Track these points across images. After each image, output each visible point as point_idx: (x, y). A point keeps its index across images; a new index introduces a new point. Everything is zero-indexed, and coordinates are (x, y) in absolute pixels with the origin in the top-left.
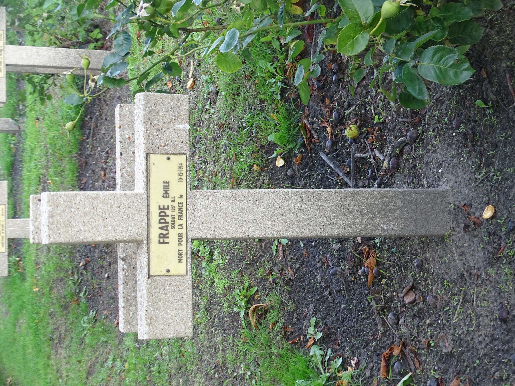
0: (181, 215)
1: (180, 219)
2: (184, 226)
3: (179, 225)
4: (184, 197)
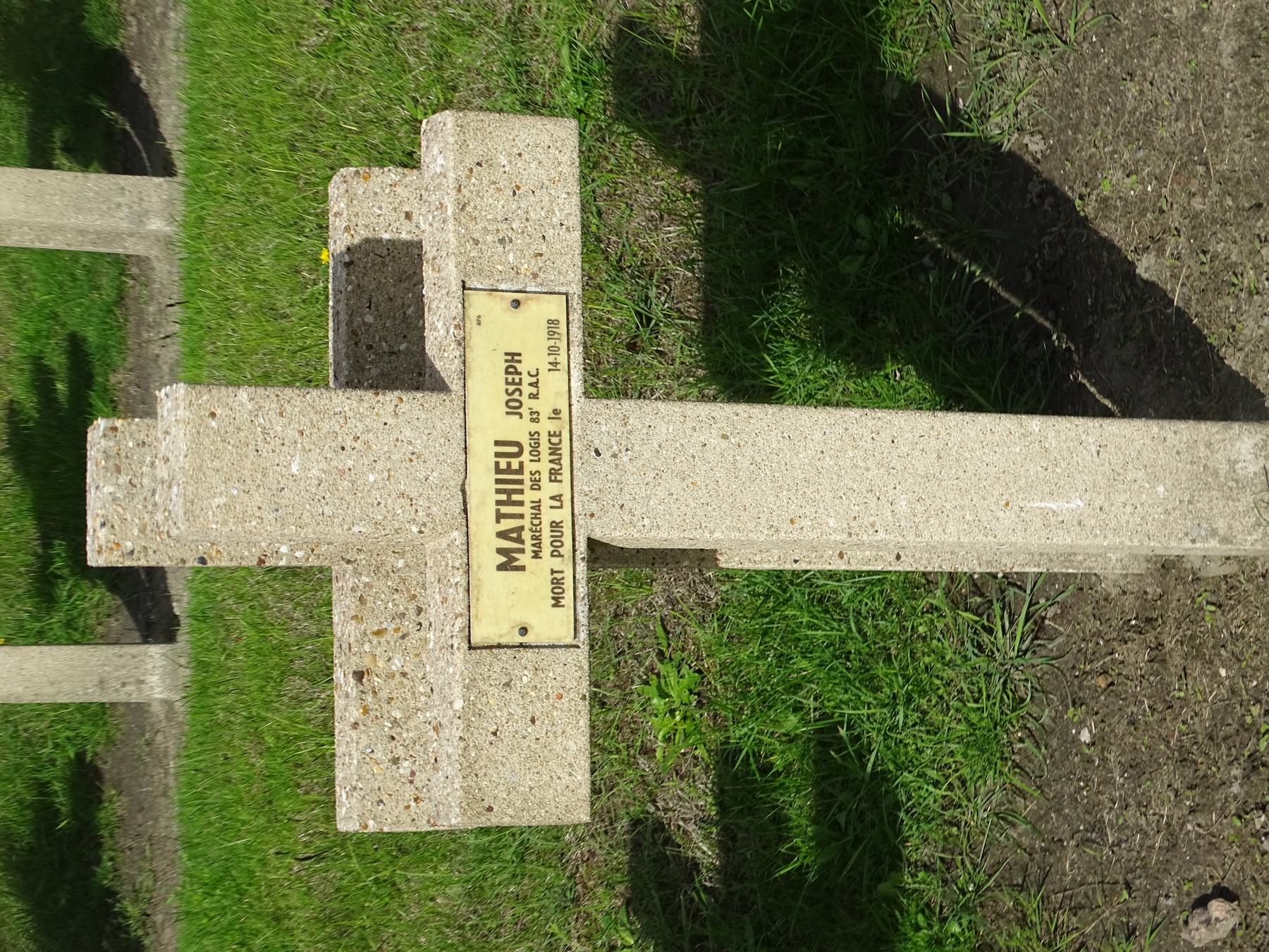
0: (557, 467)
1: (556, 481)
2: (566, 499)
3: (552, 498)
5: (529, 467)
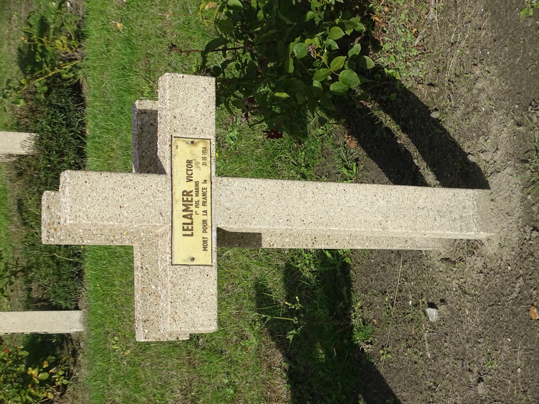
1: (205, 205)
3: (203, 212)
5: (195, 199)
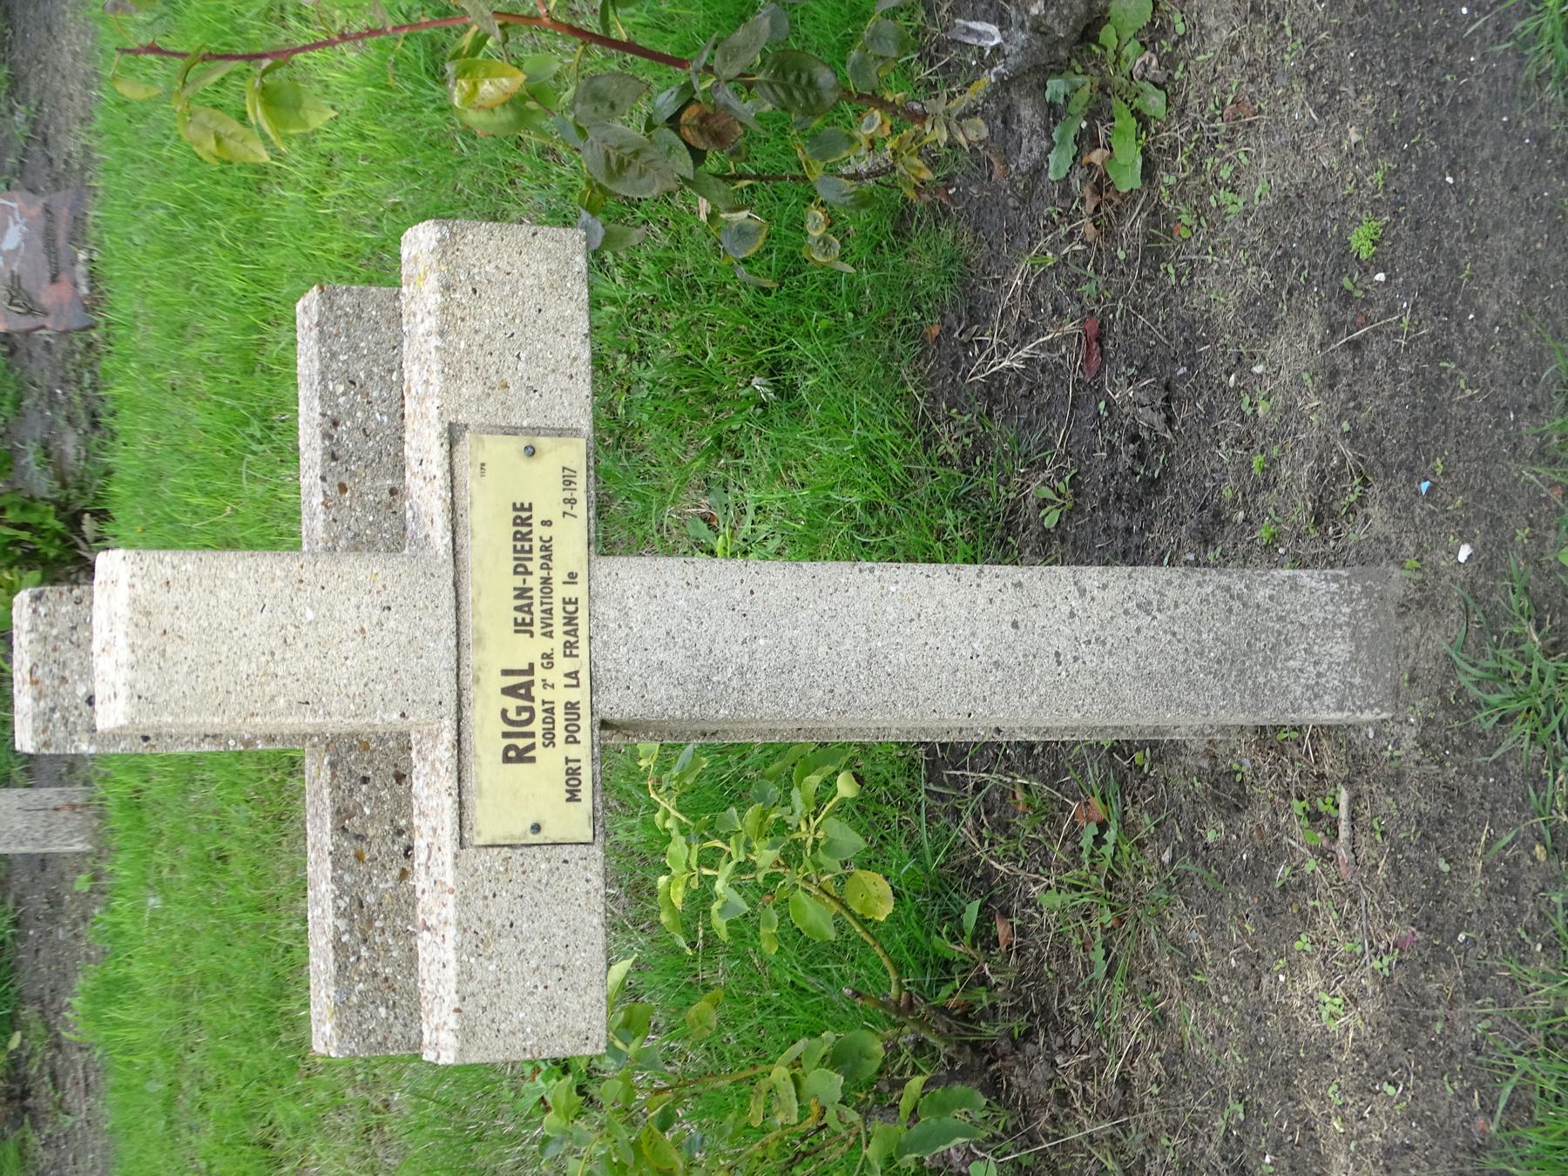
0: (573, 639)
1: (571, 655)
2: (584, 677)
3: (568, 675)
4: (582, 578)
